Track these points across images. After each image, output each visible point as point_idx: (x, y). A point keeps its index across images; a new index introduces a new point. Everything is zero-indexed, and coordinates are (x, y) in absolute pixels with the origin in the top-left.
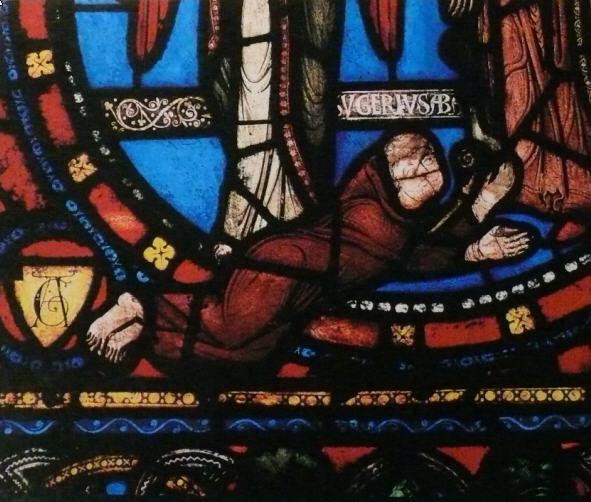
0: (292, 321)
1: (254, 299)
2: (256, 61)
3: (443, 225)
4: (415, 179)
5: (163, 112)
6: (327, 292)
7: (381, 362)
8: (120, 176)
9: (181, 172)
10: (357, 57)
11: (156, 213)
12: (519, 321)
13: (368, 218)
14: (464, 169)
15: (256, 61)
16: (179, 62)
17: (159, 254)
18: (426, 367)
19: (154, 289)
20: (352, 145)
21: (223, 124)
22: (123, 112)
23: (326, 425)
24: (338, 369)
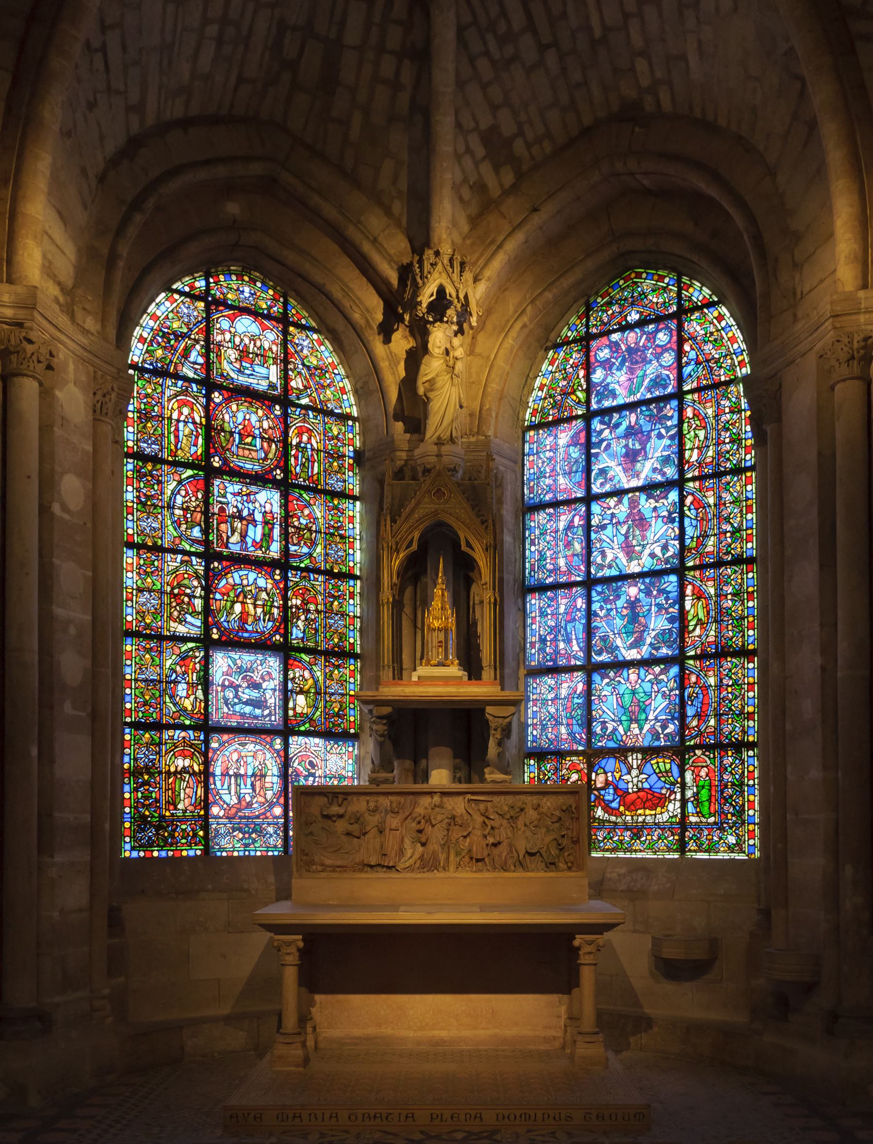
0: (236, 813)
1: (233, 811)
2: (233, 787)
3: (249, 805)
4: (248, 799)
5: (224, 792)
6: (239, 810)
7: (244, 817)
8: (221, 798)
9: (226, 798)
10: (242, 786)
11: (224, 802)
12: (257, 813)
13: (243, 803)
14: (253, 797)
15: (233, 787)
16: (226, 786)
17: (225, 806)
18: (249, 818)
19: (225, 810)
20: (242, 795)
21: (230, 793)
22: (221, 792)
23: (239, 823)
24: (241, 818)
